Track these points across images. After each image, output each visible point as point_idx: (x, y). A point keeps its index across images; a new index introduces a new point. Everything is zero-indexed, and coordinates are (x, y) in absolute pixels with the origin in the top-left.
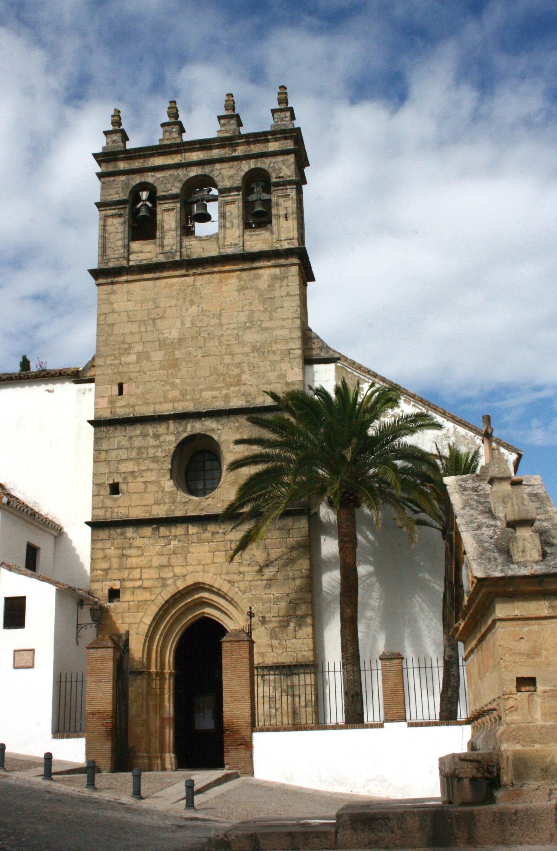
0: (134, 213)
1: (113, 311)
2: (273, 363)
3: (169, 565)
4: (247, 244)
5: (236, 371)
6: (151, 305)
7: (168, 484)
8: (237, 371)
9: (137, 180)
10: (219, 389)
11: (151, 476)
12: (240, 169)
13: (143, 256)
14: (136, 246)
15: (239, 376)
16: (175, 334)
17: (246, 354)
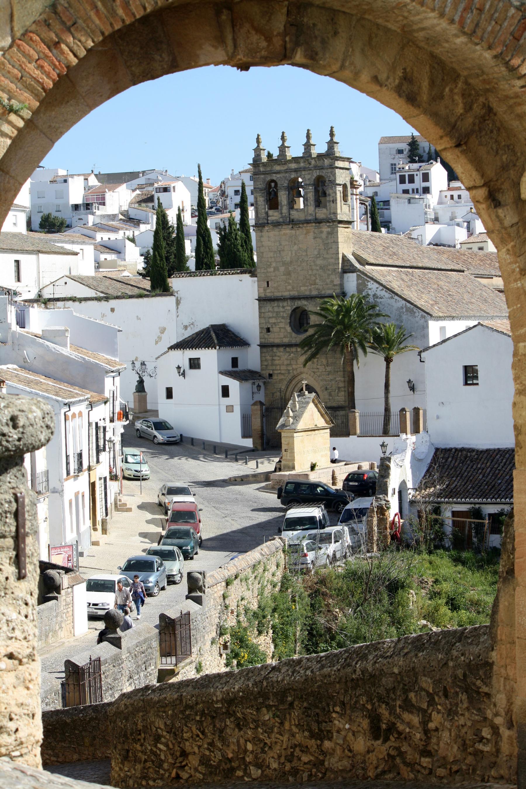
0: (269, 193)
1: (263, 246)
2: (329, 275)
3: (290, 364)
4: (317, 215)
5: (314, 278)
6: (278, 244)
7: (289, 329)
8: (314, 278)
9: (269, 178)
10: (307, 286)
11: (282, 325)
12: (312, 175)
13: (274, 218)
14: (271, 212)
15: (315, 280)
16: (288, 259)
17: (317, 270)
